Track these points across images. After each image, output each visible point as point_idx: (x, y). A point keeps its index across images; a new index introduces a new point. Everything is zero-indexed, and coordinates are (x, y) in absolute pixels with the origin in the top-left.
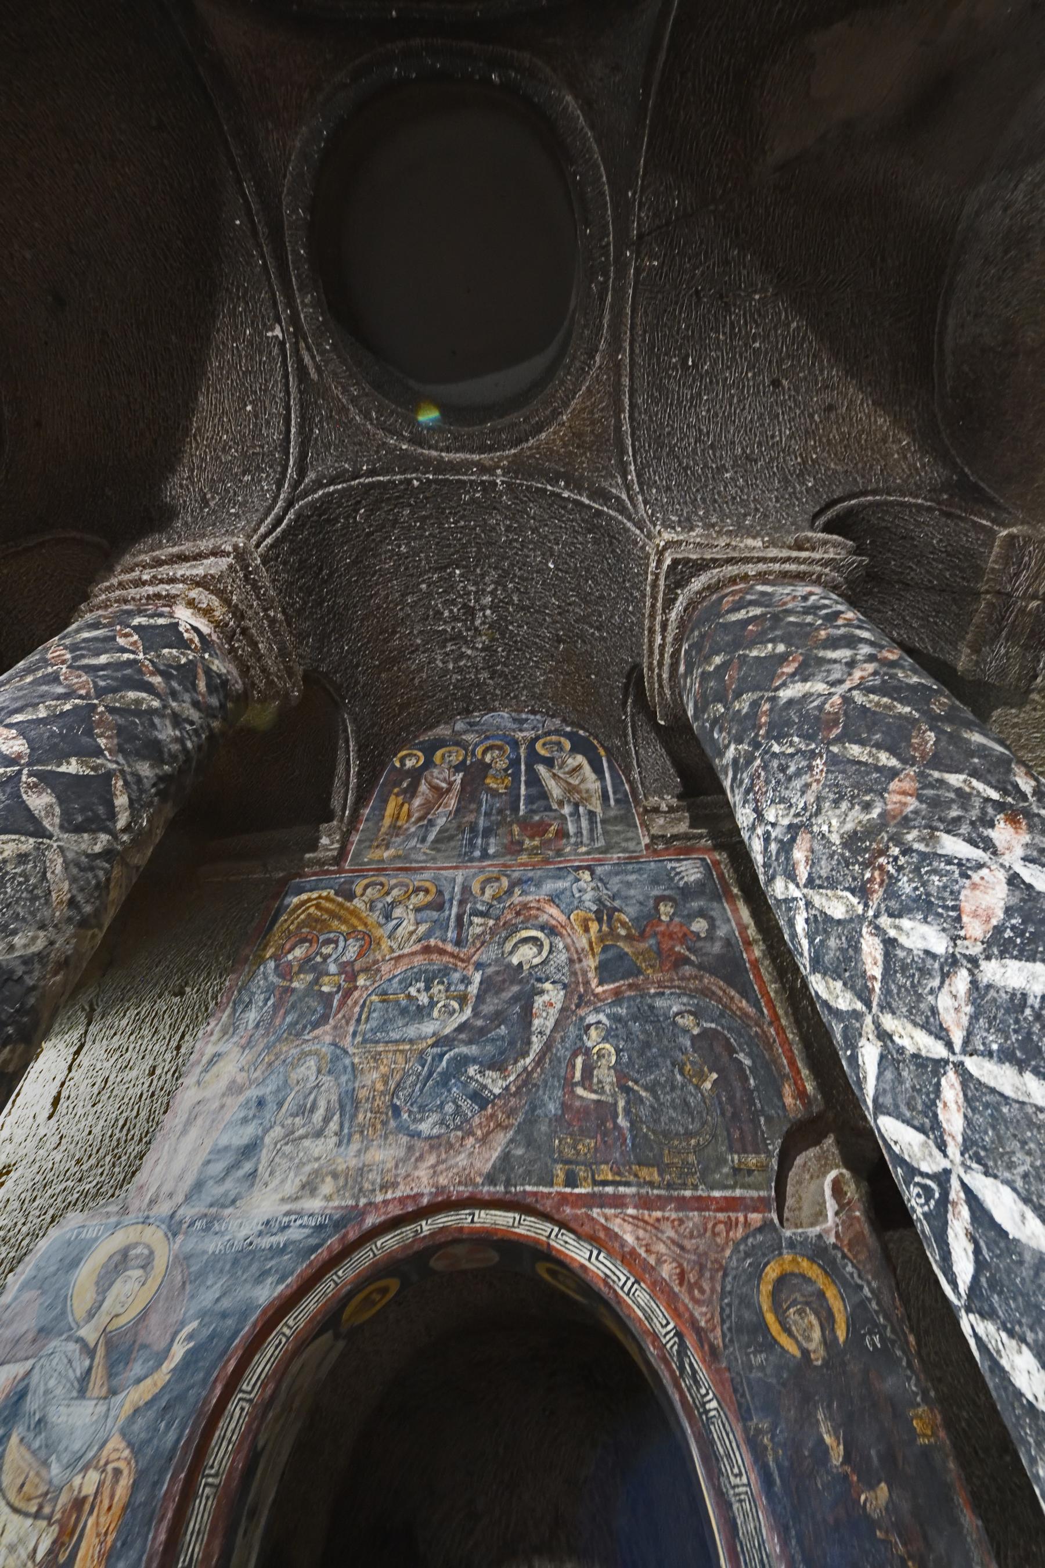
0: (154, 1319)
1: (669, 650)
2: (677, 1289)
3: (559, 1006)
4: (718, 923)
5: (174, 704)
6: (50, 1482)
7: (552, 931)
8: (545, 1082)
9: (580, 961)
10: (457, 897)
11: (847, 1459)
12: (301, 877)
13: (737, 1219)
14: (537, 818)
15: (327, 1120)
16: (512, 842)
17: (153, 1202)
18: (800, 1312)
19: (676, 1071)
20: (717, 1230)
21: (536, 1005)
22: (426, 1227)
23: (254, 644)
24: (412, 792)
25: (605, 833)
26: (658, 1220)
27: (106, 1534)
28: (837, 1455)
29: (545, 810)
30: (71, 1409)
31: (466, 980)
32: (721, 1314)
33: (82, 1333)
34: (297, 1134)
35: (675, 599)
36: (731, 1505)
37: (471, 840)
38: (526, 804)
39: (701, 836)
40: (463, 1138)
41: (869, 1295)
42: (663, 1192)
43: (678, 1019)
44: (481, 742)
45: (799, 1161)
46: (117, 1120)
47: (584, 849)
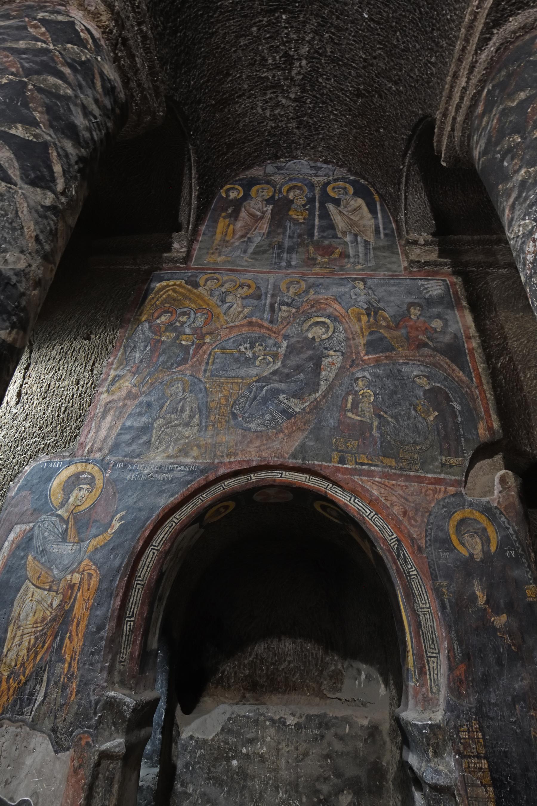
0: (99, 509)
1: (471, 91)
2: (401, 519)
3: (339, 365)
4: (450, 323)
5: (82, 96)
6: (54, 577)
7: (335, 319)
8: (328, 407)
9: (354, 339)
10: (271, 292)
11: (487, 602)
12: (160, 270)
13: (440, 489)
14: (327, 242)
15: (191, 417)
16: (308, 258)
17: (90, 452)
18: (471, 536)
19: (412, 409)
20: (427, 493)
21: (323, 363)
22: (254, 477)
23: (132, 57)
25: (376, 256)
26: (393, 485)
27: (88, 599)
28: (482, 599)
29: (333, 237)
30: (59, 547)
31: (277, 345)
32: (426, 532)
33: (59, 512)
34: (173, 423)
35: (490, 39)
36: (419, 615)
37: (279, 254)
38: (318, 232)
39: (445, 264)
40: (276, 433)
41: (512, 533)
42: (397, 472)
43: (417, 379)
44: (286, 183)
45: (478, 465)
46: (60, 408)
47: (360, 267)
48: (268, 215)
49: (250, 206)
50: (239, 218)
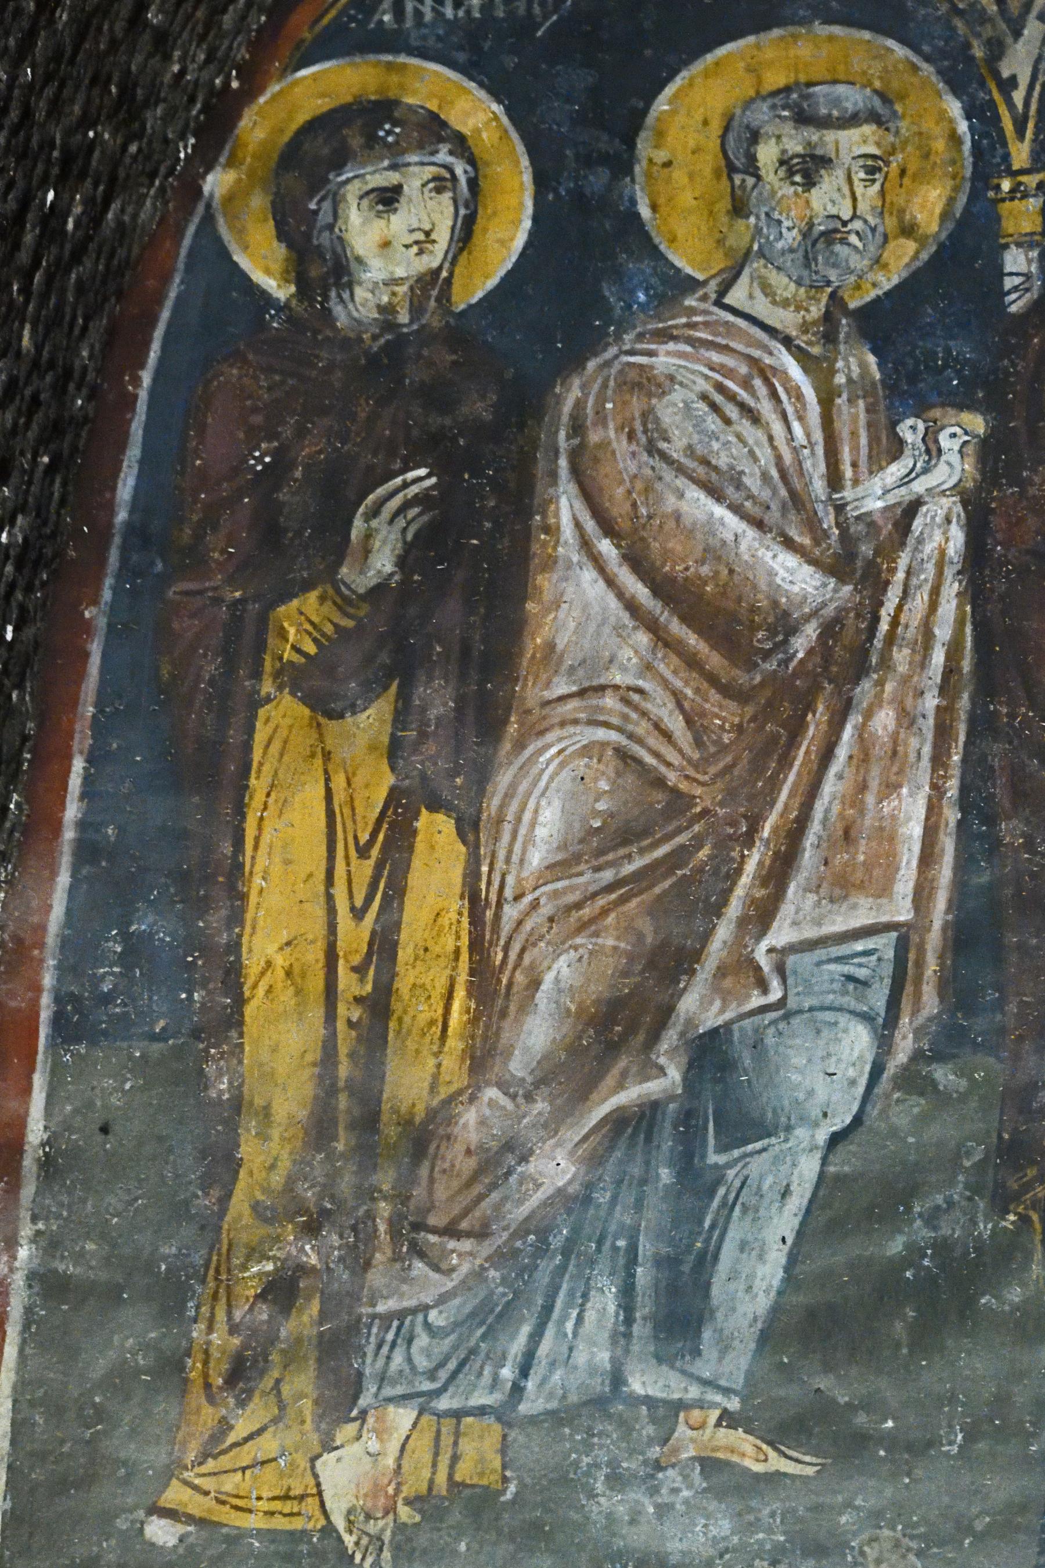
24: (454, 648)
48: (931, 601)
49: (652, 440)
50: (532, 692)
